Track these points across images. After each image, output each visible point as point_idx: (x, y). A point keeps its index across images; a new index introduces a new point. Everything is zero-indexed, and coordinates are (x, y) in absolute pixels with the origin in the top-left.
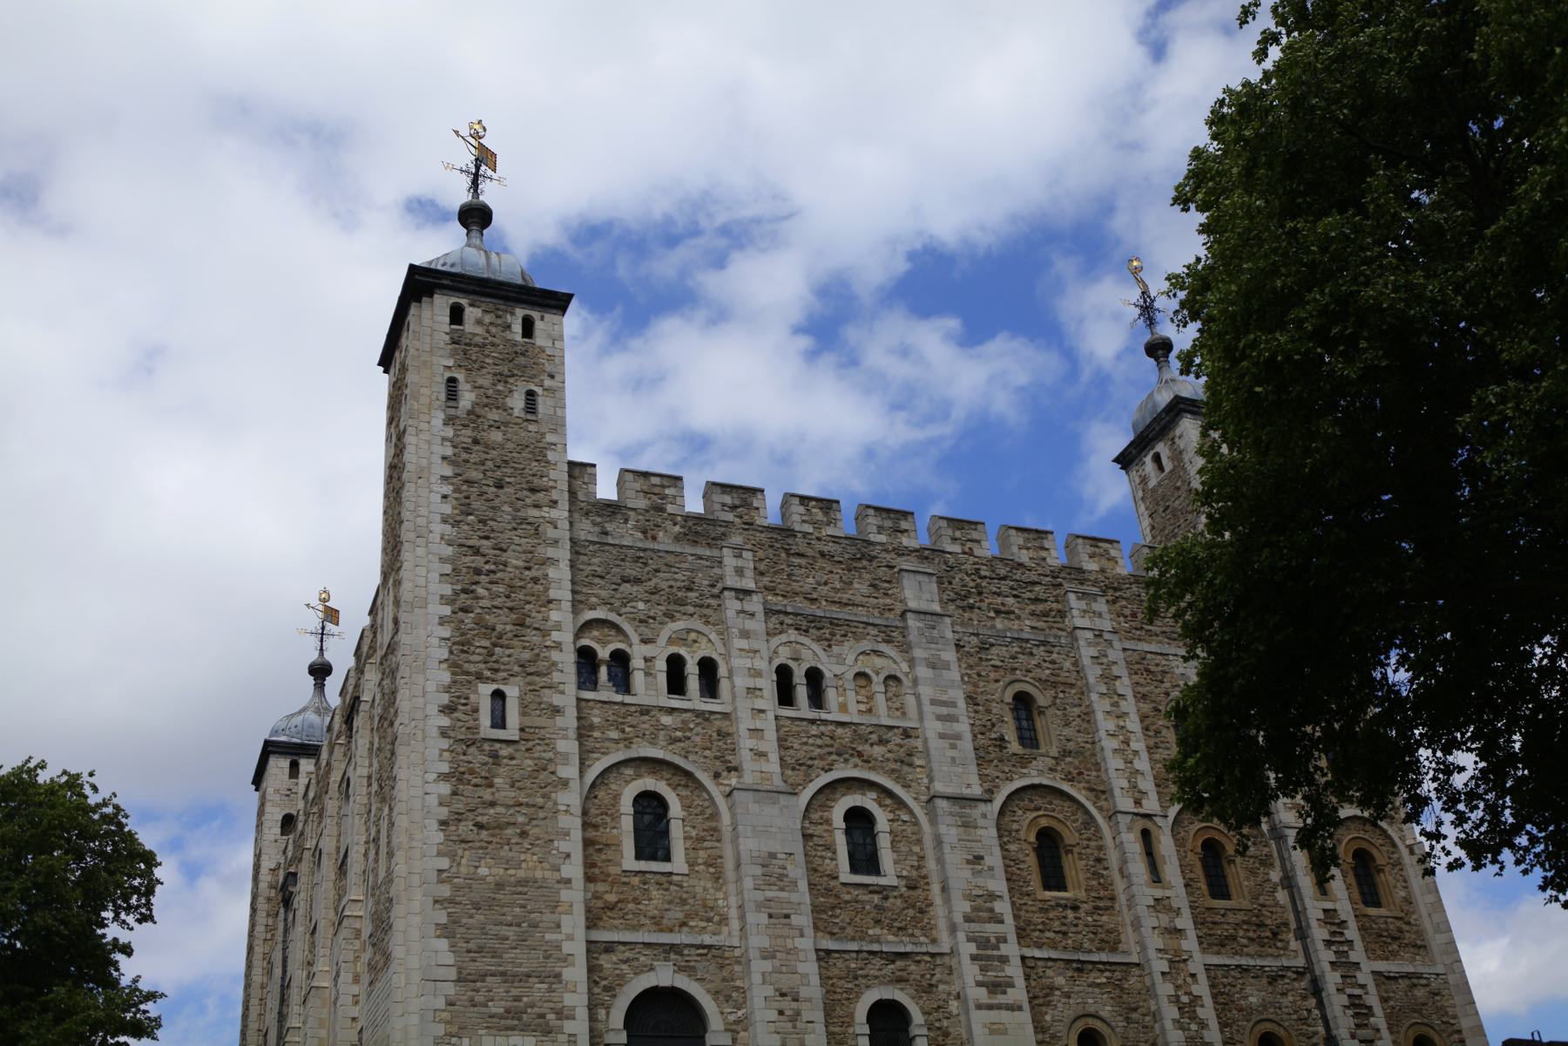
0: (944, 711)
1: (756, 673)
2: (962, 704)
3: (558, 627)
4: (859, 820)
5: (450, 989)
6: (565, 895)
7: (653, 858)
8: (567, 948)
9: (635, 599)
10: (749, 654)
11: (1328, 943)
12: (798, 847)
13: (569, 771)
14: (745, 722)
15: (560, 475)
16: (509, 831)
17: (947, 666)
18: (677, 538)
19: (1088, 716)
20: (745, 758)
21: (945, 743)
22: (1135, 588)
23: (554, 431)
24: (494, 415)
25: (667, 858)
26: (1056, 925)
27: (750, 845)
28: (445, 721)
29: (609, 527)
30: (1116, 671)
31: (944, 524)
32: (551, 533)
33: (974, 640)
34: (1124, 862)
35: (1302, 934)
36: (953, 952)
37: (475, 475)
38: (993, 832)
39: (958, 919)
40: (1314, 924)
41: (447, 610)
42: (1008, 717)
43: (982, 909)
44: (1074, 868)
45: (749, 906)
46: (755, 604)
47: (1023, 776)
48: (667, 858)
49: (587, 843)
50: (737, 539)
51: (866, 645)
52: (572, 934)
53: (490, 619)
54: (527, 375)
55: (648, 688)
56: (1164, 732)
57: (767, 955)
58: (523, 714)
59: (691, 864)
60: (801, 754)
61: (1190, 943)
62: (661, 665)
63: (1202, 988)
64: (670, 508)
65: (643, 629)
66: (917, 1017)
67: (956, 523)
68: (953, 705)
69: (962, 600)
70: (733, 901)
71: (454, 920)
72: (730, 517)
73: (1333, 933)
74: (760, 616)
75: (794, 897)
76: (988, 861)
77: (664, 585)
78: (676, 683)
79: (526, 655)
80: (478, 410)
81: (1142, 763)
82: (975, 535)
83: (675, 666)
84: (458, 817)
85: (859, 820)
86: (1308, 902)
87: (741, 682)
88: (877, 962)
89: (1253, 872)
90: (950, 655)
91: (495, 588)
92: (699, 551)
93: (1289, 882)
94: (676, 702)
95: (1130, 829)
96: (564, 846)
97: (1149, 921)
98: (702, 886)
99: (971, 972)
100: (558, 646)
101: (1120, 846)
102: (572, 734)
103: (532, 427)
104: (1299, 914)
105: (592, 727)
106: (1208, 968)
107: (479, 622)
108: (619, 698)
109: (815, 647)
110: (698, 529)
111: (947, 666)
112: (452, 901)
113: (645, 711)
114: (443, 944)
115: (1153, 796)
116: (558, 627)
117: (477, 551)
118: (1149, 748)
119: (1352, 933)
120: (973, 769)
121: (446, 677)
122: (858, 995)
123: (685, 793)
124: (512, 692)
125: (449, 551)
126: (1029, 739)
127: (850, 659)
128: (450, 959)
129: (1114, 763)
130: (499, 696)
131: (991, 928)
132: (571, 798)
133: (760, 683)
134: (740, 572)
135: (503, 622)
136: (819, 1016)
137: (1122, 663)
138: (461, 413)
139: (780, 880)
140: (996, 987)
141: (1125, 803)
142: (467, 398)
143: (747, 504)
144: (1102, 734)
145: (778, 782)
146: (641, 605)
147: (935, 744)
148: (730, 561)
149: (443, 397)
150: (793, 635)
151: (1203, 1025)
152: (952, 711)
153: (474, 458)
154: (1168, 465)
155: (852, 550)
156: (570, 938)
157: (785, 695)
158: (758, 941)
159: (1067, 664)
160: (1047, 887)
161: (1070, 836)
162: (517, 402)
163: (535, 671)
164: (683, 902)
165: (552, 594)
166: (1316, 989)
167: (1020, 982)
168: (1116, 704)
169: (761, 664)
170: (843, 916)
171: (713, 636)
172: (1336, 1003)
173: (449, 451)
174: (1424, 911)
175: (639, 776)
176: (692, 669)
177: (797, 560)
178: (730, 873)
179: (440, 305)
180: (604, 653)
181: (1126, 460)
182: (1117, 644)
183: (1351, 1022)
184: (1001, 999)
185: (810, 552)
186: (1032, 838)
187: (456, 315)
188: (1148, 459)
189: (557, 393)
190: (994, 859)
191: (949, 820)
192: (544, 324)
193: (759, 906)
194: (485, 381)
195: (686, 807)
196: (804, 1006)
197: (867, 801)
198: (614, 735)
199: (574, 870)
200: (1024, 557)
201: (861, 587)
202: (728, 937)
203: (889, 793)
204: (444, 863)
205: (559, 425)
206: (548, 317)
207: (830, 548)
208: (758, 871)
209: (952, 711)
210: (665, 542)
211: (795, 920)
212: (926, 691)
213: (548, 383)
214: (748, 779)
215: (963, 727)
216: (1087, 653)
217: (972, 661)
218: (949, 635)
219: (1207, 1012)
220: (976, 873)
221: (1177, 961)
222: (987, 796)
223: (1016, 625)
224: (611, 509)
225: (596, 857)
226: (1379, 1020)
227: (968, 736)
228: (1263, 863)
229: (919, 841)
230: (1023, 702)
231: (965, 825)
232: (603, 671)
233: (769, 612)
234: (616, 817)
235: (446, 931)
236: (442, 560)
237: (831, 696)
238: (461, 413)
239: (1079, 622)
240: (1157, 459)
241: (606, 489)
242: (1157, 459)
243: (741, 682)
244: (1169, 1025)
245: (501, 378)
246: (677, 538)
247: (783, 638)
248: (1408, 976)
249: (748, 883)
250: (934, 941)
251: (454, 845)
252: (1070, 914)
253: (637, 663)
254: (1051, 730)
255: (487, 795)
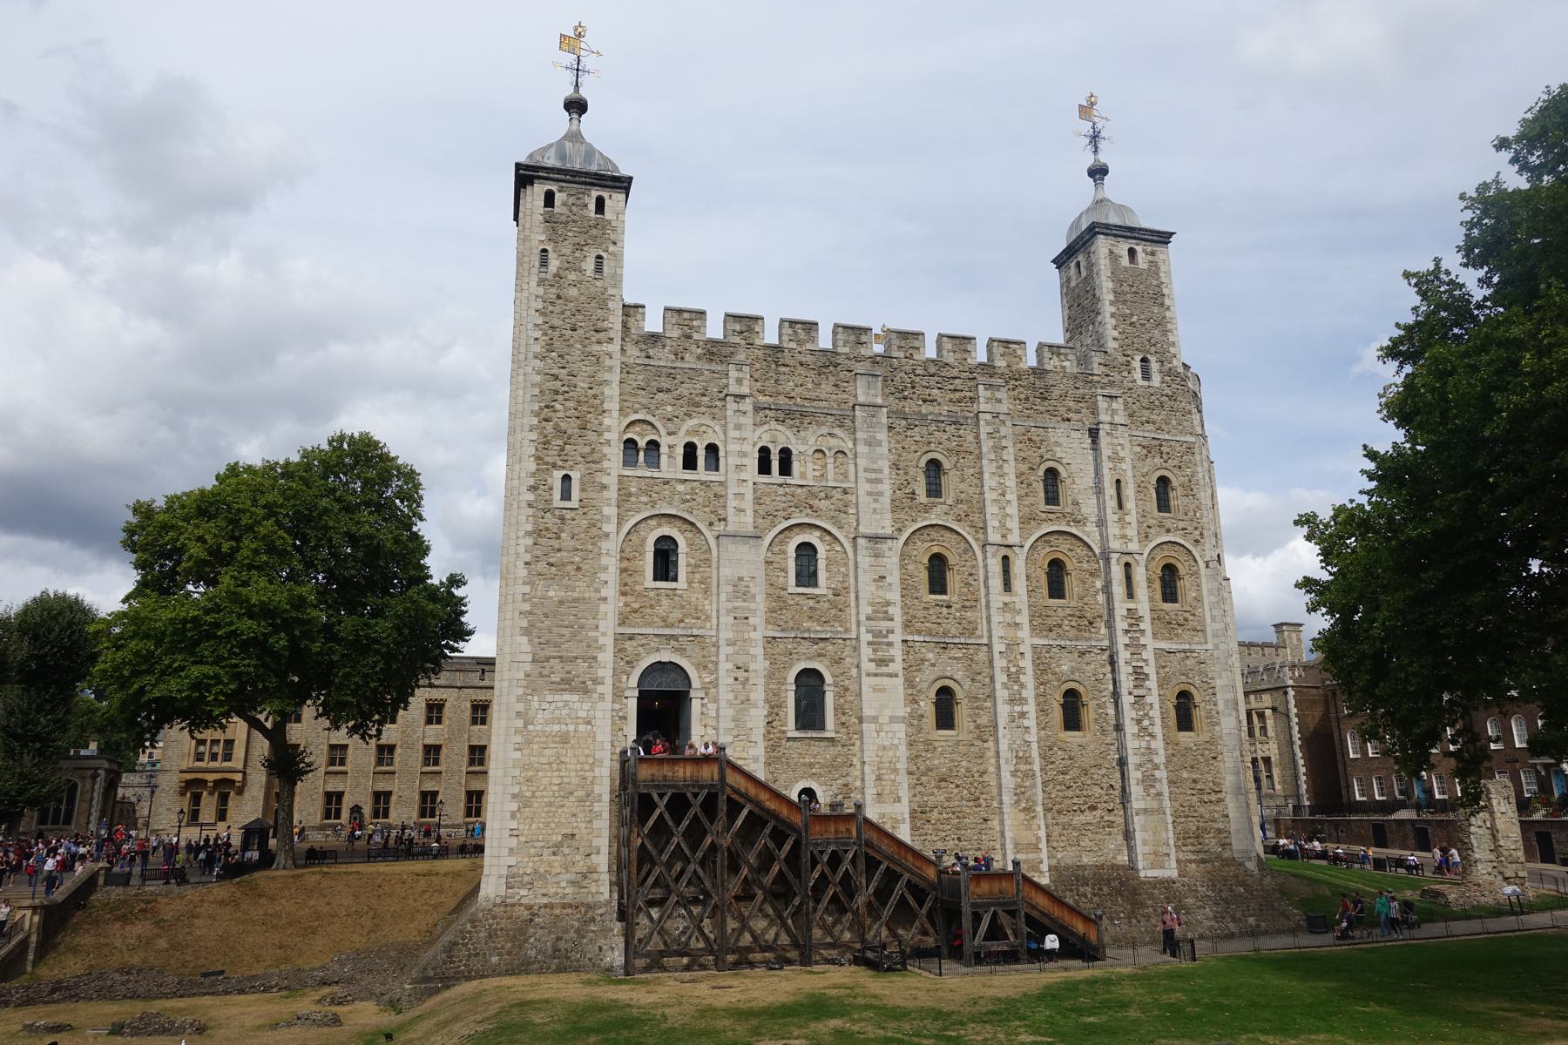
0: (873, 476)
1: (743, 454)
2: (887, 471)
3: (609, 429)
4: (806, 550)
5: (528, 667)
6: (603, 608)
7: (667, 580)
8: (602, 641)
9: (667, 404)
10: (741, 439)
11: (1127, 631)
12: (760, 574)
13: (610, 528)
14: (733, 489)
15: (615, 321)
16: (570, 567)
17: (879, 444)
18: (699, 358)
19: (980, 474)
20: (731, 511)
21: (870, 499)
22: (1032, 378)
23: (615, 286)
24: (572, 276)
25: (675, 579)
26: (933, 618)
27: (727, 572)
28: (530, 497)
29: (651, 352)
30: (1004, 443)
31: (894, 336)
32: (608, 362)
33: (904, 423)
34: (986, 578)
35: (1110, 625)
36: (858, 639)
37: (556, 322)
38: (896, 560)
39: (862, 618)
40: (1118, 618)
41: (535, 421)
42: (922, 479)
43: (881, 611)
44: (953, 580)
45: (722, 612)
46: (747, 405)
47: (924, 519)
48: (675, 579)
49: (623, 570)
50: (741, 357)
51: (824, 430)
52: (607, 627)
53: (563, 425)
54: (598, 236)
55: (670, 464)
56: (1035, 484)
57: (730, 643)
58: (583, 490)
59: (690, 583)
60: (770, 508)
61: (1024, 633)
62: (680, 451)
63: (1027, 663)
64: (696, 336)
65: (669, 424)
66: (828, 679)
67: (904, 335)
68: (881, 471)
69: (900, 393)
70: (714, 607)
71: (532, 625)
72: (737, 340)
73: (1131, 625)
74: (750, 414)
75: (753, 606)
76: (889, 579)
77: (686, 393)
78: (690, 462)
79: (587, 450)
80: (562, 273)
81: (1013, 510)
82: (916, 344)
83: (690, 449)
84: (537, 559)
85: (806, 550)
86: (1117, 604)
87: (732, 461)
88: (806, 643)
89: (1084, 583)
90: (882, 435)
91: (568, 404)
92: (713, 367)
93: (1107, 589)
94: (689, 475)
95: (994, 555)
96: (603, 576)
97: (996, 618)
98: (696, 596)
99: (866, 652)
100: (608, 443)
101: (985, 566)
102: (614, 502)
103: (598, 284)
104: (1111, 610)
105: (630, 495)
106: (1034, 647)
107: (556, 427)
108: (649, 474)
109: (789, 433)
110: (715, 351)
111: (879, 444)
112: (530, 613)
113: (666, 482)
114: (525, 639)
115: (1016, 532)
116: (609, 429)
117: (556, 377)
118: (1020, 498)
119: (1146, 625)
120: (889, 515)
121: (533, 467)
122: (791, 666)
123: (689, 535)
124: (575, 476)
125: (538, 378)
126: (934, 491)
127: (812, 441)
128: (528, 648)
129: (991, 509)
130: (567, 478)
131: (884, 625)
132: (611, 546)
133: (745, 461)
134: (739, 381)
135: (572, 427)
136: (761, 681)
137: (1010, 437)
138: (549, 276)
139: (746, 595)
140: (882, 662)
141: (994, 537)
142: (554, 264)
143: (750, 330)
144: (986, 488)
145: (750, 528)
146: (669, 408)
147: (863, 498)
148: (733, 374)
149: (537, 264)
150: (773, 424)
151: (1022, 686)
152: (879, 476)
153: (557, 309)
154: (1084, 274)
155: (824, 360)
156: (604, 634)
157: (764, 468)
158: (726, 634)
159: (970, 438)
160: (932, 591)
161: (952, 559)
162: (589, 265)
163: (593, 460)
164: (683, 607)
165: (606, 406)
166: (1112, 662)
167: (899, 659)
168: (1000, 467)
169: (747, 448)
170: (787, 615)
171: (717, 428)
172: (1125, 671)
173: (540, 305)
174: (1207, 608)
175: (660, 525)
176: (701, 454)
177: (782, 369)
178: (714, 590)
179: (537, 192)
180: (642, 443)
181: (1060, 262)
182: (1009, 423)
183: (1132, 684)
184: (884, 670)
185: (792, 362)
186: (926, 561)
187: (549, 199)
188: (1073, 265)
189: (618, 257)
190: (894, 578)
191: (865, 552)
192: (613, 200)
193: (728, 611)
194: (567, 251)
195: (690, 545)
196: (751, 675)
197: (813, 538)
198: (645, 499)
199: (610, 591)
200: (950, 358)
201: (827, 387)
202: (708, 631)
203: (829, 533)
204: (527, 589)
205: (617, 281)
206: (615, 196)
207: (809, 359)
208: (730, 589)
209: (879, 476)
210: (690, 361)
211: (752, 621)
212: (862, 462)
213: (612, 248)
214: (731, 528)
215: (886, 488)
216: (984, 429)
217: (900, 438)
218: (884, 420)
219: (1028, 678)
220: (878, 588)
221: (1012, 645)
222: (896, 534)
223: (936, 410)
224: (654, 338)
225: (629, 580)
226: (1152, 683)
227: (888, 493)
228: (1091, 574)
229: (846, 564)
230: (934, 467)
231: (876, 556)
232: (642, 454)
233: (758, 408)
234: (642, 554)
235: (526, 632)
236: (533, 386)
237: (796, 466)
238: (549, 276)
239: (983, 407)
240: (1078, 265)
241: (653, 322)
242: (1078, 265)
243: (732, 461)
244: (998, 686)
245: (579, 247)
246: (699, 358)
247: (766, 427)
248: (1184, 651)
249: (723, 597)
250: (847, 631)
251: (534, 577)
252: (945, 610)
253: (664, 449)
254: (951, 483)
255: (556, 544)
